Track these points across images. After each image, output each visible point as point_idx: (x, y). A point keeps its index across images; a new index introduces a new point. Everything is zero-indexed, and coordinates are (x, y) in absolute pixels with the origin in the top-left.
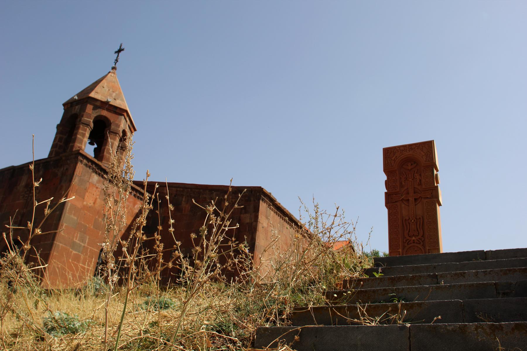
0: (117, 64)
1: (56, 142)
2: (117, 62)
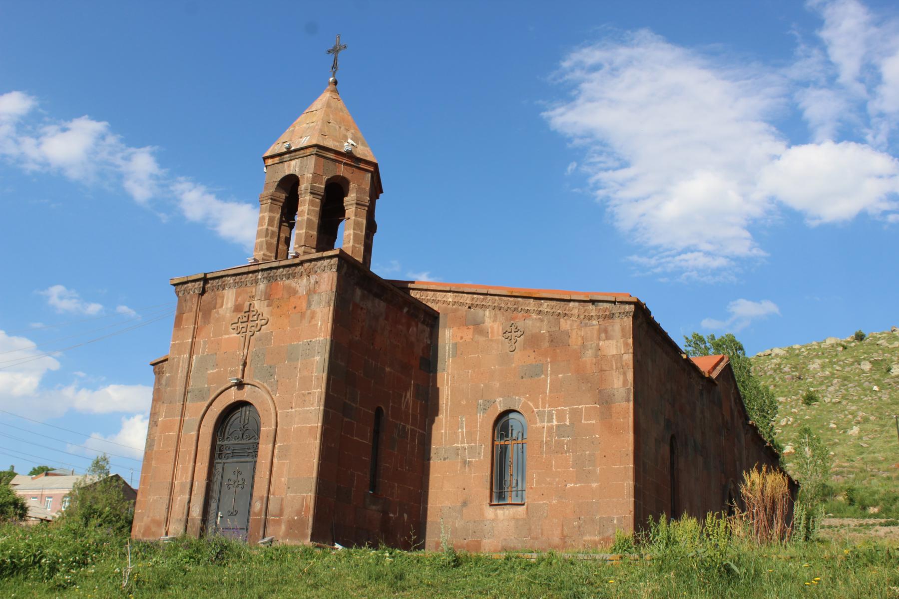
0: (336, 74)
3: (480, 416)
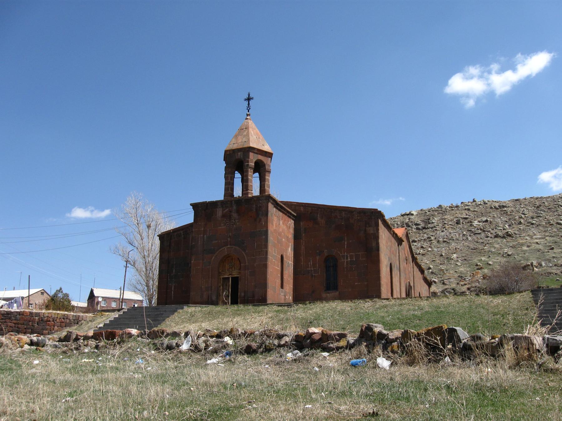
1: (229, 181)
2: (250, 109)
3: (318, 258)
